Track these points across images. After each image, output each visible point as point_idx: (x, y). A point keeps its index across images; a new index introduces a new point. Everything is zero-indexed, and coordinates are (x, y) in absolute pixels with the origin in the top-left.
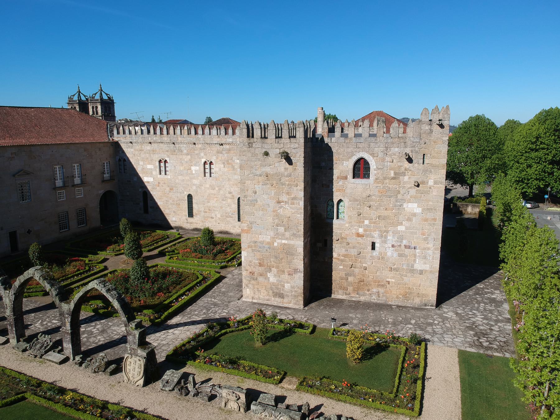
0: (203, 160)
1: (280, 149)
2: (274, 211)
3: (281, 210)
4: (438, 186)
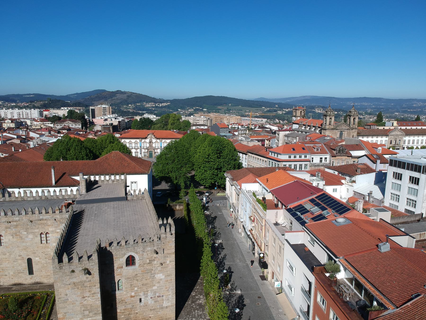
1: (82, 267)
2: (81, 303)
3: (86, 301)
4: (172, 263)
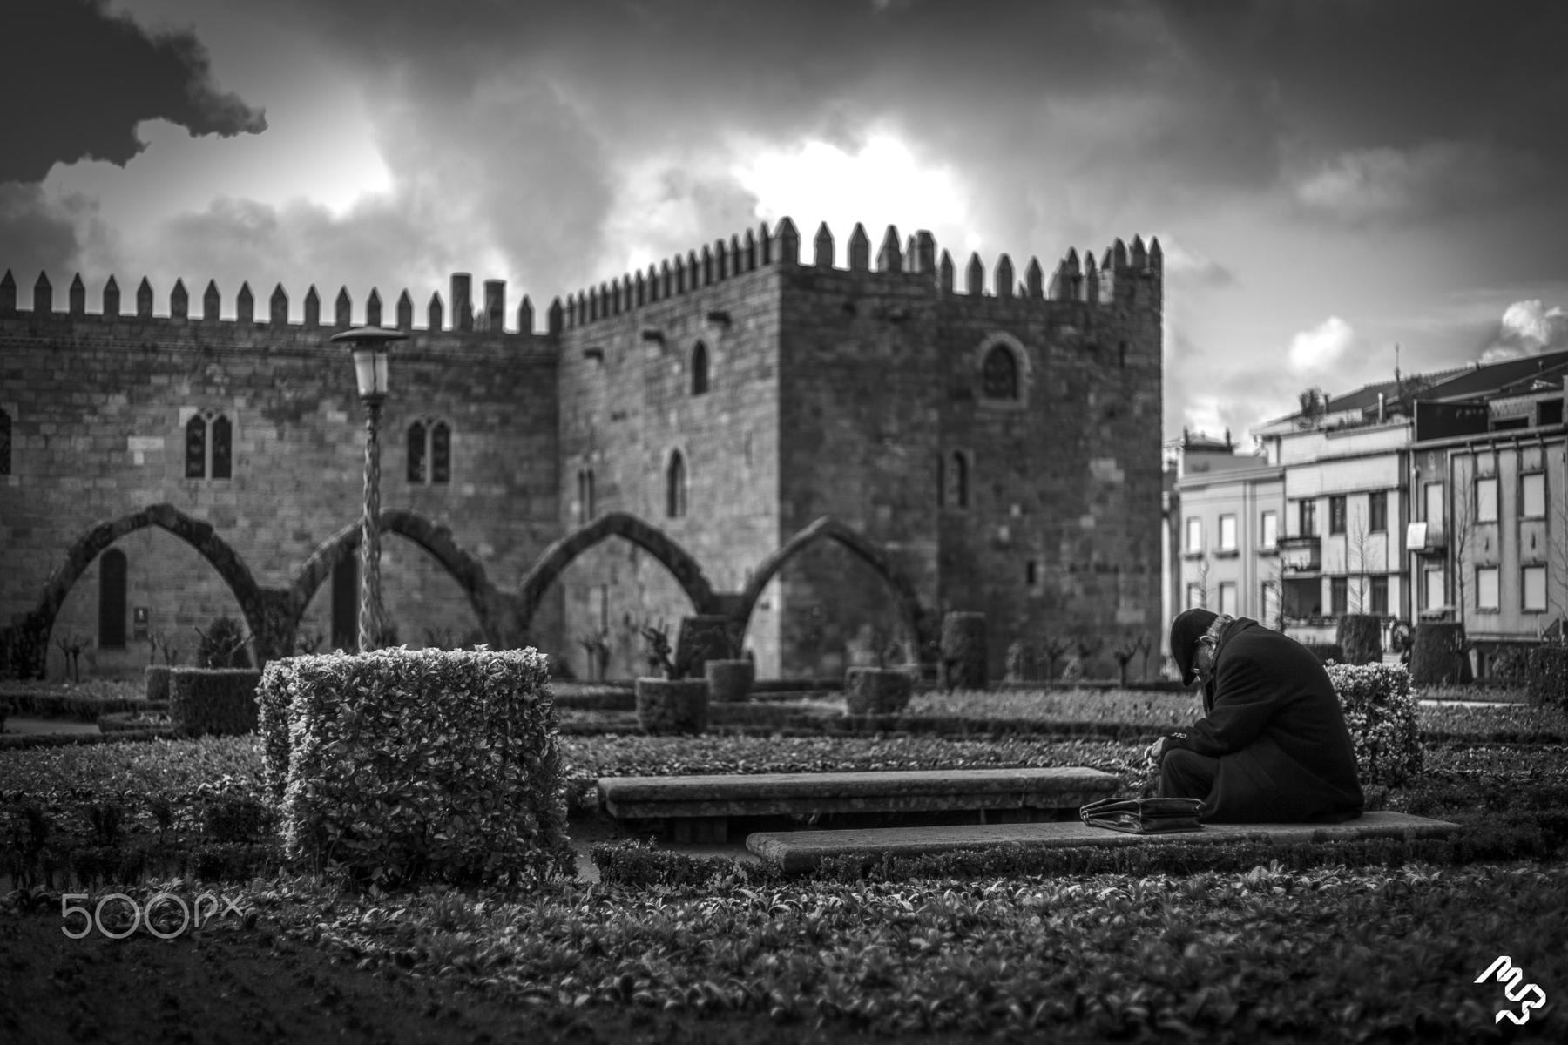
0: (186, 413)
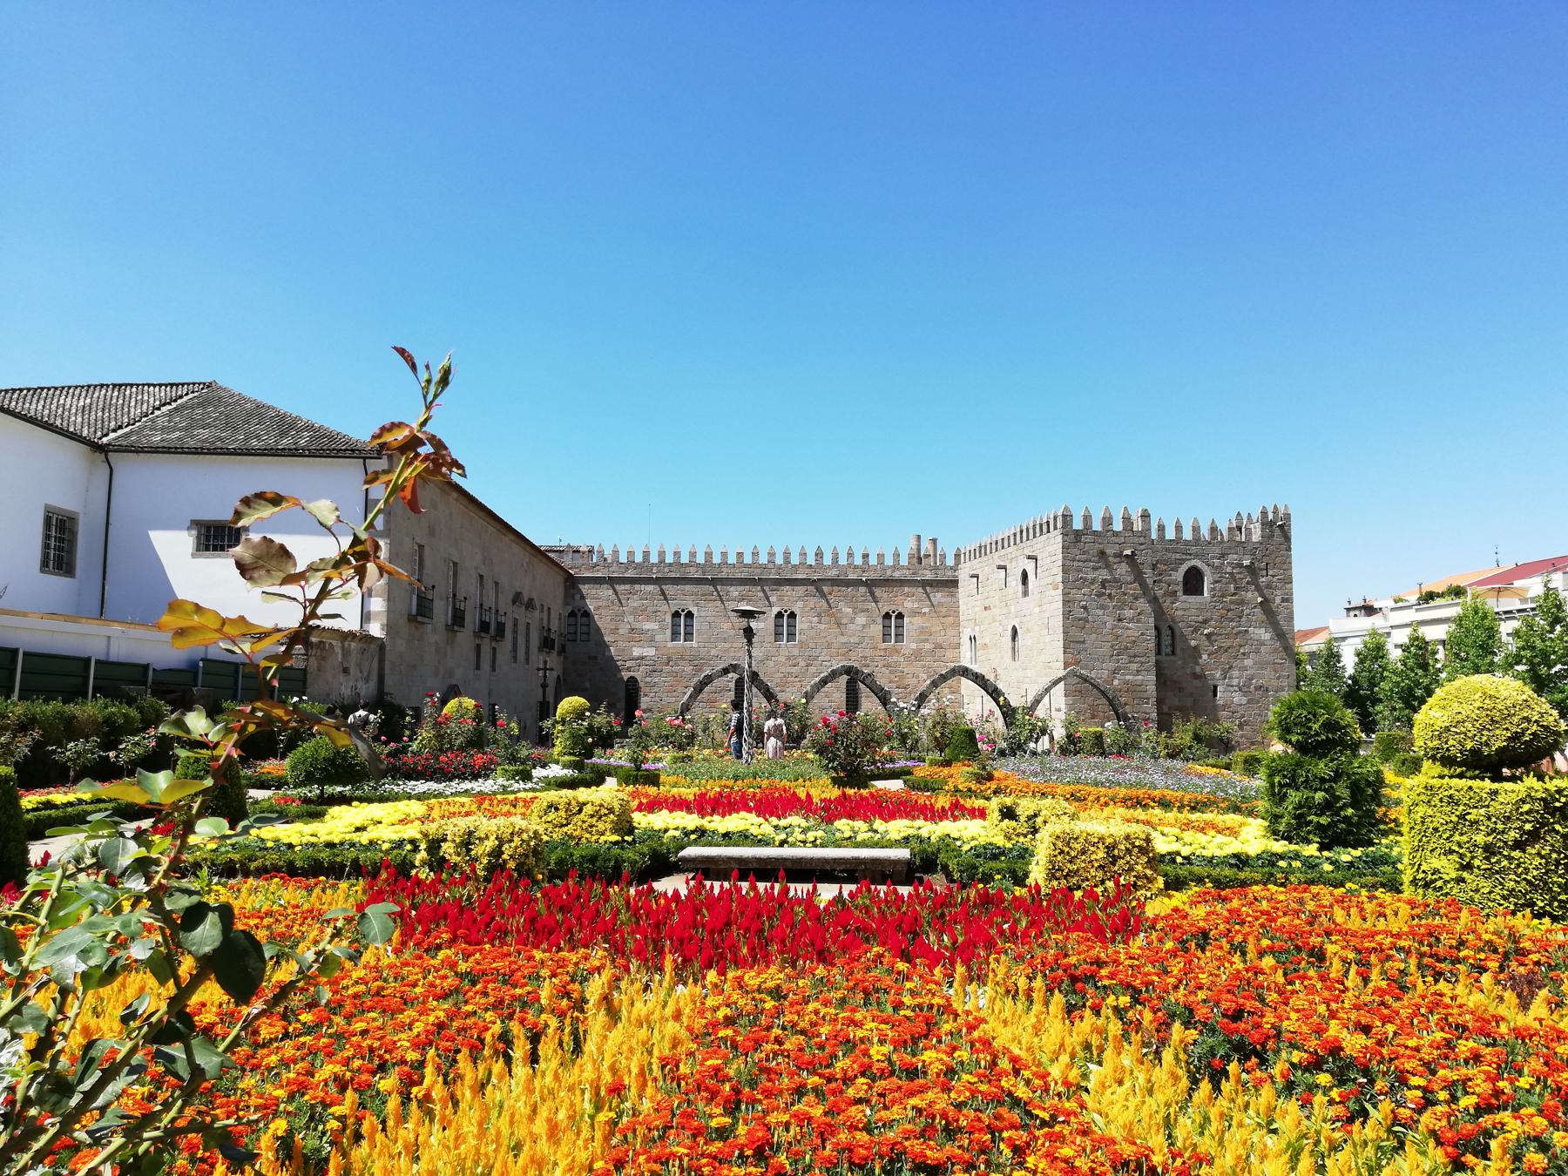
0: (775, 610)
